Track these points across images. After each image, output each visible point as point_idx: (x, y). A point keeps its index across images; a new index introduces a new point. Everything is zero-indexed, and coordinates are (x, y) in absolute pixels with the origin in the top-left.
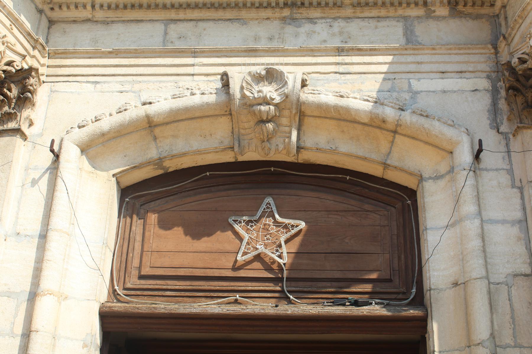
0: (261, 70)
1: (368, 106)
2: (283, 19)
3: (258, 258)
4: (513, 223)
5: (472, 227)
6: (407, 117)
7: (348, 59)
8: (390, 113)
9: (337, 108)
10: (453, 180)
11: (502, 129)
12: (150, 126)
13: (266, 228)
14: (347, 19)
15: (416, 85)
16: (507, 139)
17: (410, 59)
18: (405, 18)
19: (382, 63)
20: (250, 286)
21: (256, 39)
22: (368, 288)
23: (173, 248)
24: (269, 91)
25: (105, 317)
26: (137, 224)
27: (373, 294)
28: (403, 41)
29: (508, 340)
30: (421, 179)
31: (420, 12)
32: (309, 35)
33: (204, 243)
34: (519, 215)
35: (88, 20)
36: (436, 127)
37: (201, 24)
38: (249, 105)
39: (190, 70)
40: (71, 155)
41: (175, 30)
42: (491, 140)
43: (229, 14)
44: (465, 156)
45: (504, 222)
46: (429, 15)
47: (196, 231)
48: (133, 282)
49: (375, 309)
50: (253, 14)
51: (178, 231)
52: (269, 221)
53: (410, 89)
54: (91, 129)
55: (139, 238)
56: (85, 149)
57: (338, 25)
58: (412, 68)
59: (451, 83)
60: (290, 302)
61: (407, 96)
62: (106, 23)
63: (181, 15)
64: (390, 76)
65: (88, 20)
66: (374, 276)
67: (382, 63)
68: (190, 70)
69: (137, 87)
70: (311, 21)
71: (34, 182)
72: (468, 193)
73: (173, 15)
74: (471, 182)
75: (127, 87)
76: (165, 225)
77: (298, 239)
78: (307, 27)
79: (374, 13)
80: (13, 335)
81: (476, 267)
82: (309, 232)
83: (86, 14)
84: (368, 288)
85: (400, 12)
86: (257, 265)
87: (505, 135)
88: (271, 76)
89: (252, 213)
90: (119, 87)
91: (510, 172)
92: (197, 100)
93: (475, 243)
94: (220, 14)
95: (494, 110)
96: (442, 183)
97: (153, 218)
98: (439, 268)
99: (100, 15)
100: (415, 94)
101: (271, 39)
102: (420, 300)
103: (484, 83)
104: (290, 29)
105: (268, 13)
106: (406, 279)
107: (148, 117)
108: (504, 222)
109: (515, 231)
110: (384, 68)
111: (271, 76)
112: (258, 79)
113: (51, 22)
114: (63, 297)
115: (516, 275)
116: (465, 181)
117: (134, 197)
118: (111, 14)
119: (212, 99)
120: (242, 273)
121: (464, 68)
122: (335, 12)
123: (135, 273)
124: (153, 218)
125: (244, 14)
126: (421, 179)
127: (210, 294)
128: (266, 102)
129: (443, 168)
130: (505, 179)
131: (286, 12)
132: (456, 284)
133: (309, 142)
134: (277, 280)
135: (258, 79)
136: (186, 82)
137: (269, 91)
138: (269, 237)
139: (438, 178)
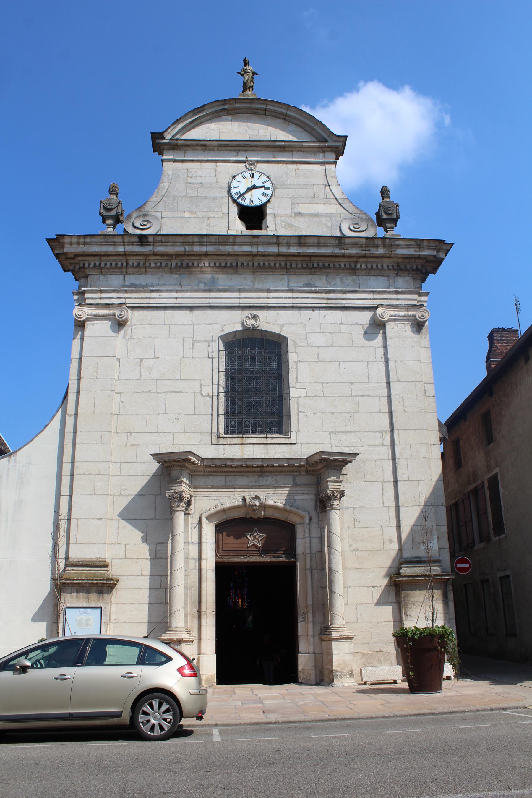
0: (254, 496)
1: (282, 506)
2: (259, 475)
3: (254, 545)
4: (318, 538)
5: (308, 540)
6: (293, 509)
7: (277, 489)
8: (288, 507)
9: (274, 506)
10: (304, 526)
11: (318, 511)
12: (224, 511)
13: (255, 536)
14: (277, 475)
15: (296, 498)
16: (318, 514)
17: (294, 489)
18: (293, 475)
19: (286, 491)
20: (252, 552)
21: (252, 482)
22: (282, 552)
23: (231, 542)
24: (257, 502)
25: (217, 563)
26: (221, 535)
27: (283, 554)
28: (292, 483)
29: (314, 568)
30: (296, 524)
31: (298, 473)
32: (266, 480)
33: (239, 541)
34: (320, 535)
35: (202, 475)
36: (300, 512)
37: (235, 477)
38: (251, 506)
39: (233, 493)
40: (204, 520)
41: (228, 478)
42: (314, 514)
43: (243, 474)
44: (307, 520)
45: (316, 538)
46: (300, 475)
47: (237, 537)
48: (221, 552)
49: (283, 559)
50: (250, 474)
51: (232, 537)
52: (256, 534)
53: (294, 499)
54: (209, 513)
55: (221, 539)
56: (207, 518)
57: (275, 477)
58: (294, 492)
59: (305, 497)
60: (263, 557)
61: (293, 501)
62: (208, 476)
63: (230, 474)
64: (288, 495)
65: (202, 475)
66: (284, 549)
67: (286, 491)
68: (233, 493)
69: (219, 498)
70: (267, 476)
71: (195, 528)
72: (307, 531)
73: (227, 474)
74: (308, 528)
75: (216, 498)
76: (228, 536)
77: (264, 539)
78: (266, 478)
79: (285, 474)
80: (195, 569)
81: (308, 551)
82: (267, 537)
83: (202, 474)
84: (282, 552)
85: (292, 474)
86: (253, 547)
87: (318, 513)
88: (257, 498)
89: (251, 531)
90: (214, 498)
91: (318, 523)
92: (237, 504)
93: (308, 544)
94: (241, 474)
95: (316, 505)
96: (301, 526)
97: (225, 533)
98: (299, 550)
99: (206, 474)
100: (295, 500)
101: (255, 482)
102: (295, 556)
103: (313, 497)
104: (261, 479)
105: (255, 474)
106: (291, 551)
107: (224, 509)
108: (316, 538)
109: (318, 540)
110: (287, 492)
111: (257, 498)
112: (253, 498)
113: (192, 476)
114: (207, 559)
115: (318, 551)
116: (307, 528)
117: (219, 528)
118: (209, 474)
119: (241, 503)
120: (249, 549)
121: (308, 492)
122: (273, 474)
123: (221, 549)
124: (225, 533)
125: (248, 474)
126: (296, 524)
127: (242, 555)
128: (256, 505)
129: (302, 522)
130: (317, 525)
131: (260, 474)
132: (303, 554)
133: (267, 514)
134: (259, 551)
135: (253, 498)
136: (233, 496)
137: (257, 502)
138: (256, 539)
139: (300, 524)
